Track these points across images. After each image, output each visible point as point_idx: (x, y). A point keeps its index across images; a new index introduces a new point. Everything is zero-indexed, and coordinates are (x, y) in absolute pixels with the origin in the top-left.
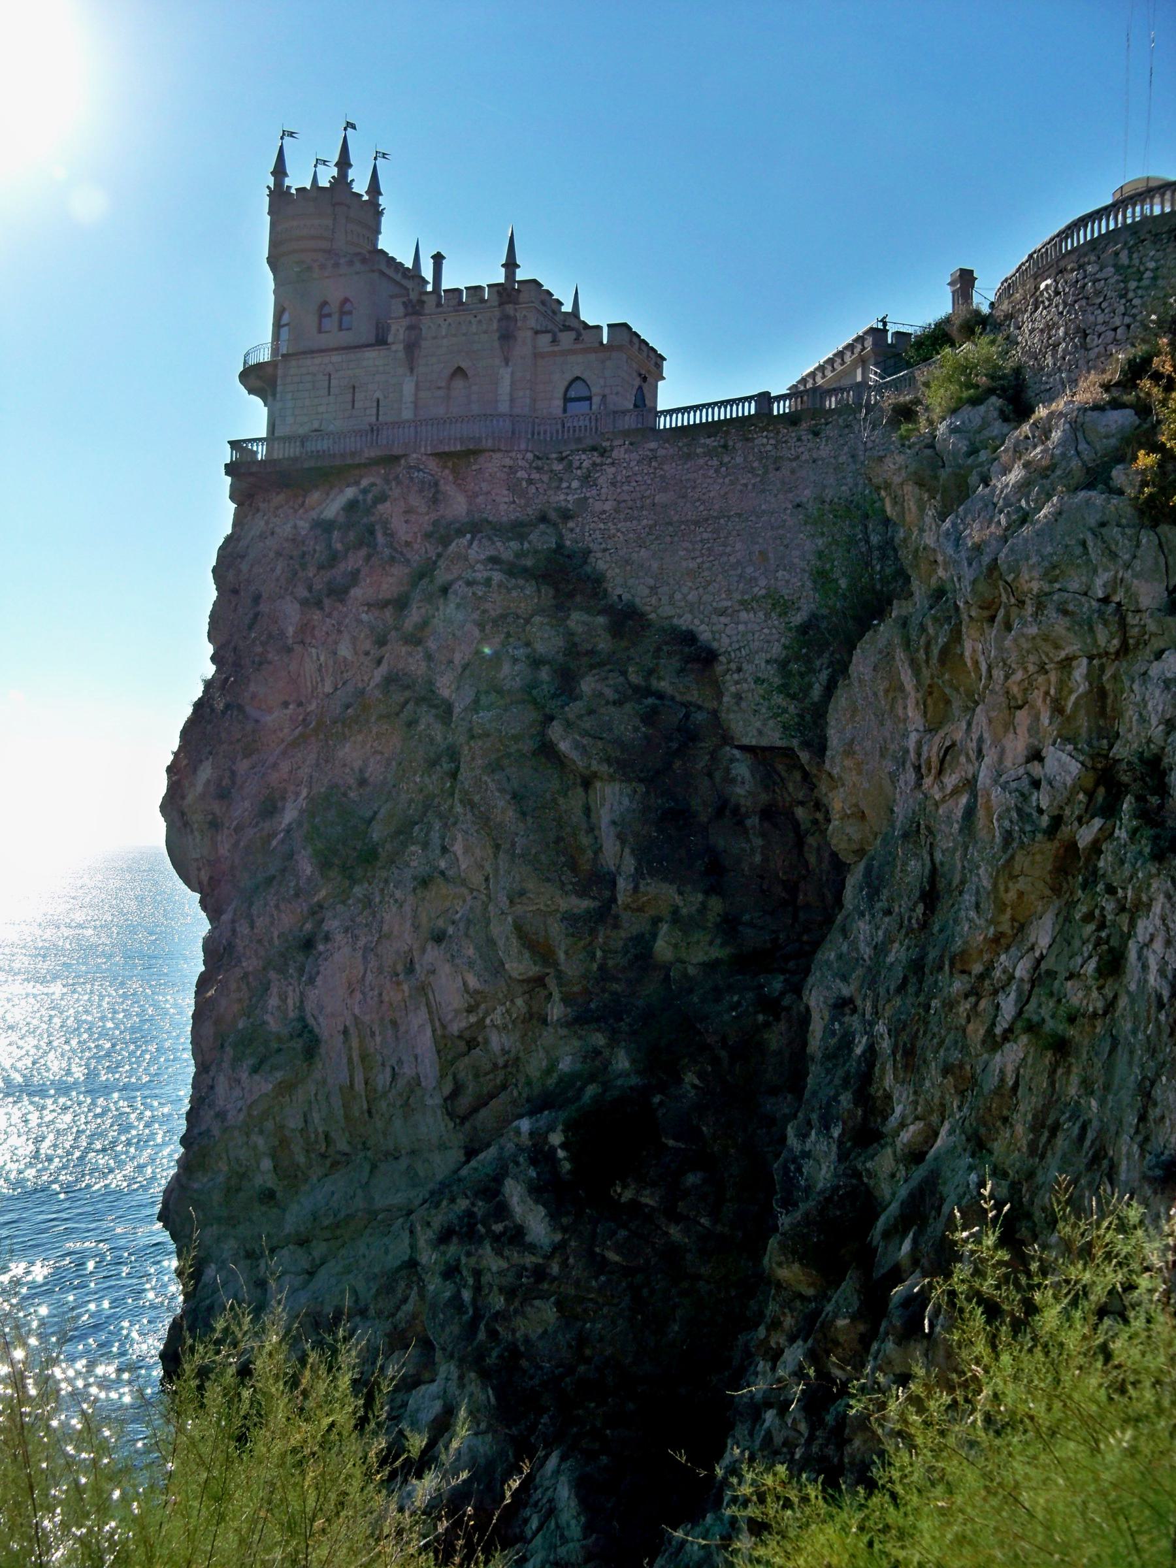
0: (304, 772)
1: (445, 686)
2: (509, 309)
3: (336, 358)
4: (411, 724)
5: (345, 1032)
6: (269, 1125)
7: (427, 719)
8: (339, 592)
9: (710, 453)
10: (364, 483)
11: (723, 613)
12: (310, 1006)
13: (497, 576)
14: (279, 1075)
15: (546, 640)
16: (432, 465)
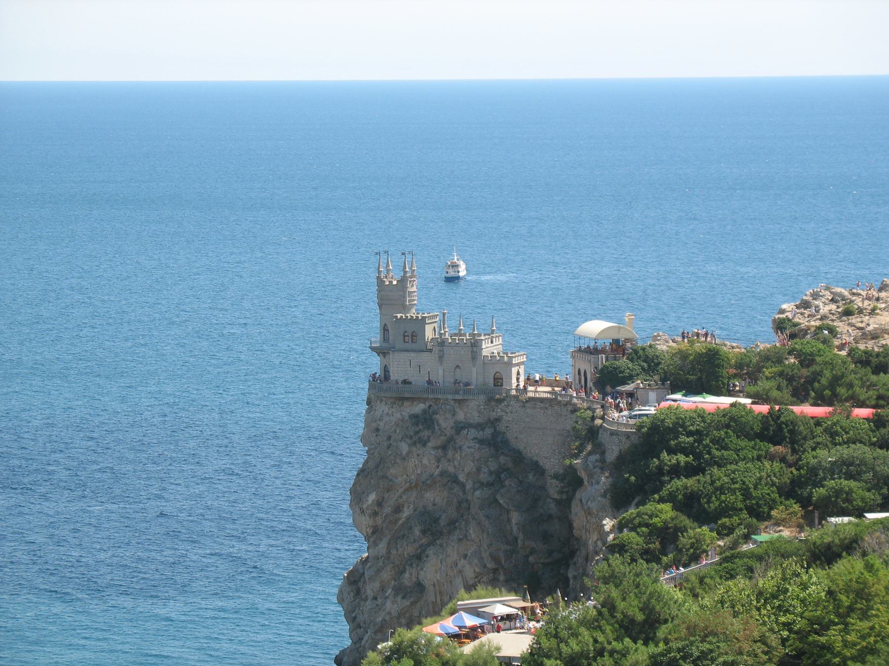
0: (412, 499)
1: (462, 478)
2: (475, 349)
3: (413, 354)
4: (451, 489)
5: (434, 585)
6: (407, 615)
7: (457, 489)
8: (424, 444)
9: (541, 408)
10: (428, 404)
11: (546, 458)
12: (421, 577)
13: (477, 445)
14: (412, 599)
15: (493, 466)
16: (452, 403)
